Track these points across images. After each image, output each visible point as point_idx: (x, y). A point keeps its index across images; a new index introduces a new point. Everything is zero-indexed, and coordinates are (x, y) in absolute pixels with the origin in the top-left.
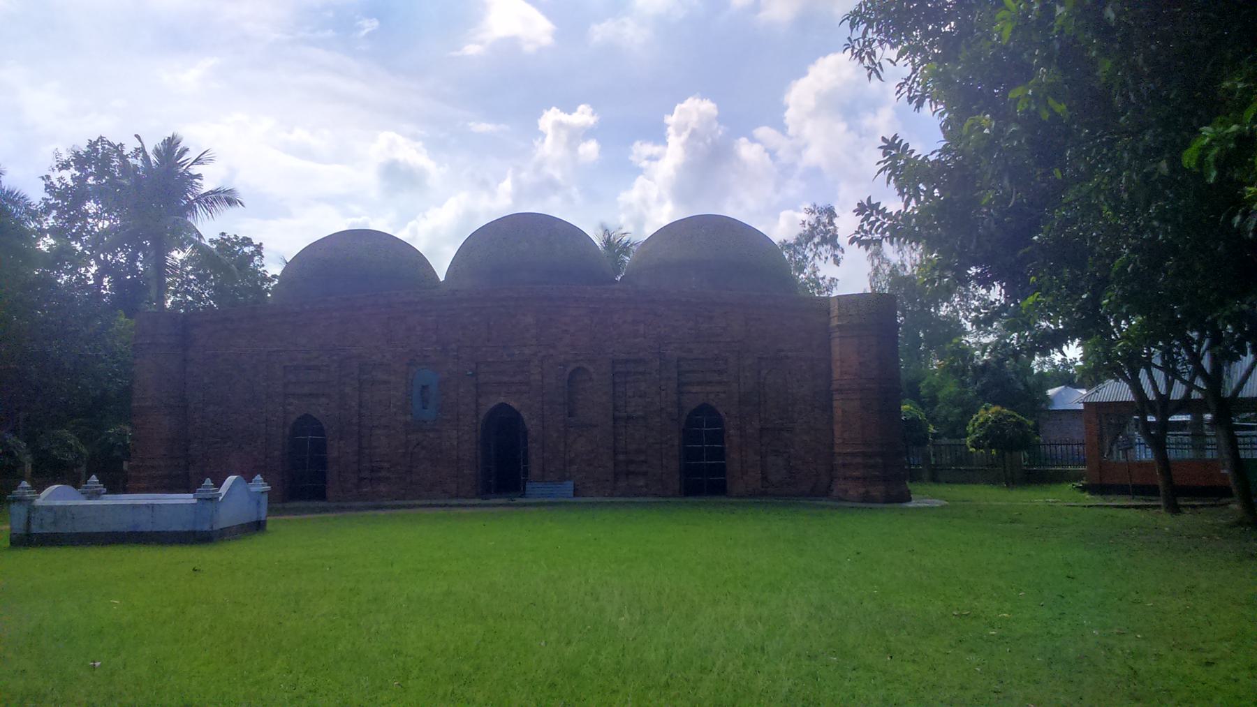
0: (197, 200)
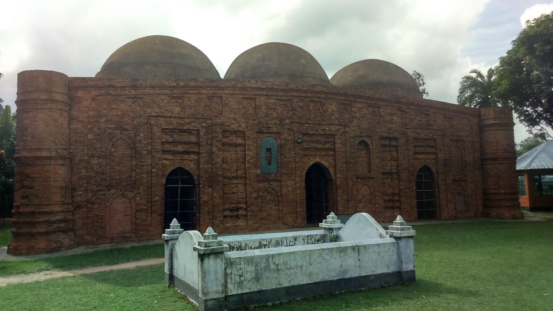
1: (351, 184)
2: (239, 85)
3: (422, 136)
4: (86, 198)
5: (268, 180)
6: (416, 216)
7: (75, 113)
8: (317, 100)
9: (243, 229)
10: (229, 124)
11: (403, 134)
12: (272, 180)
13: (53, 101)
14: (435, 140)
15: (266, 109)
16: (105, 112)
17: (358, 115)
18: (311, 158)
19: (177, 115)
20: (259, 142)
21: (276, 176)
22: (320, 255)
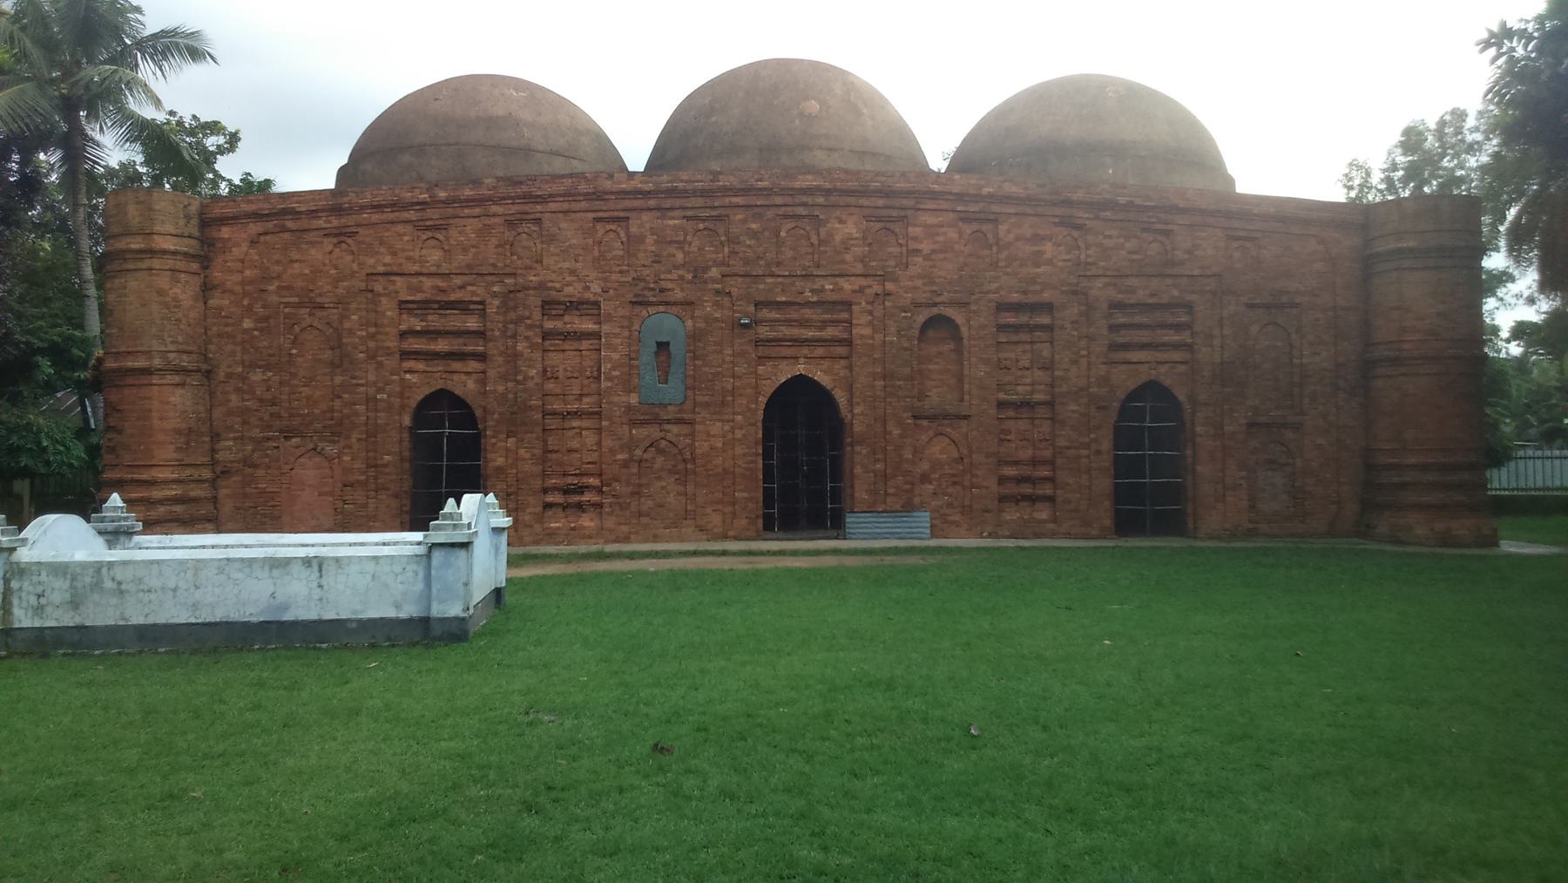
0: (141, 44)
1: (896, 432)
2: (583, 188)
3: (1141, 295)
4: (240, 455)
5: (656, 421)
6: (1108, 522)
7: (217, 275)
8: (801, 211)
9: (590, 537)
10: (558, 285)
11: (1074, 293)
12: (669, 422)
13: (152, 253)
14: (1189, 307)
15: (657, 242)
16: (278, 268)
17: (925, 247)
18: (783, 365)
19: (433, 269)
20: (636, 327)
21: (680, 411)
22: (221, 571)
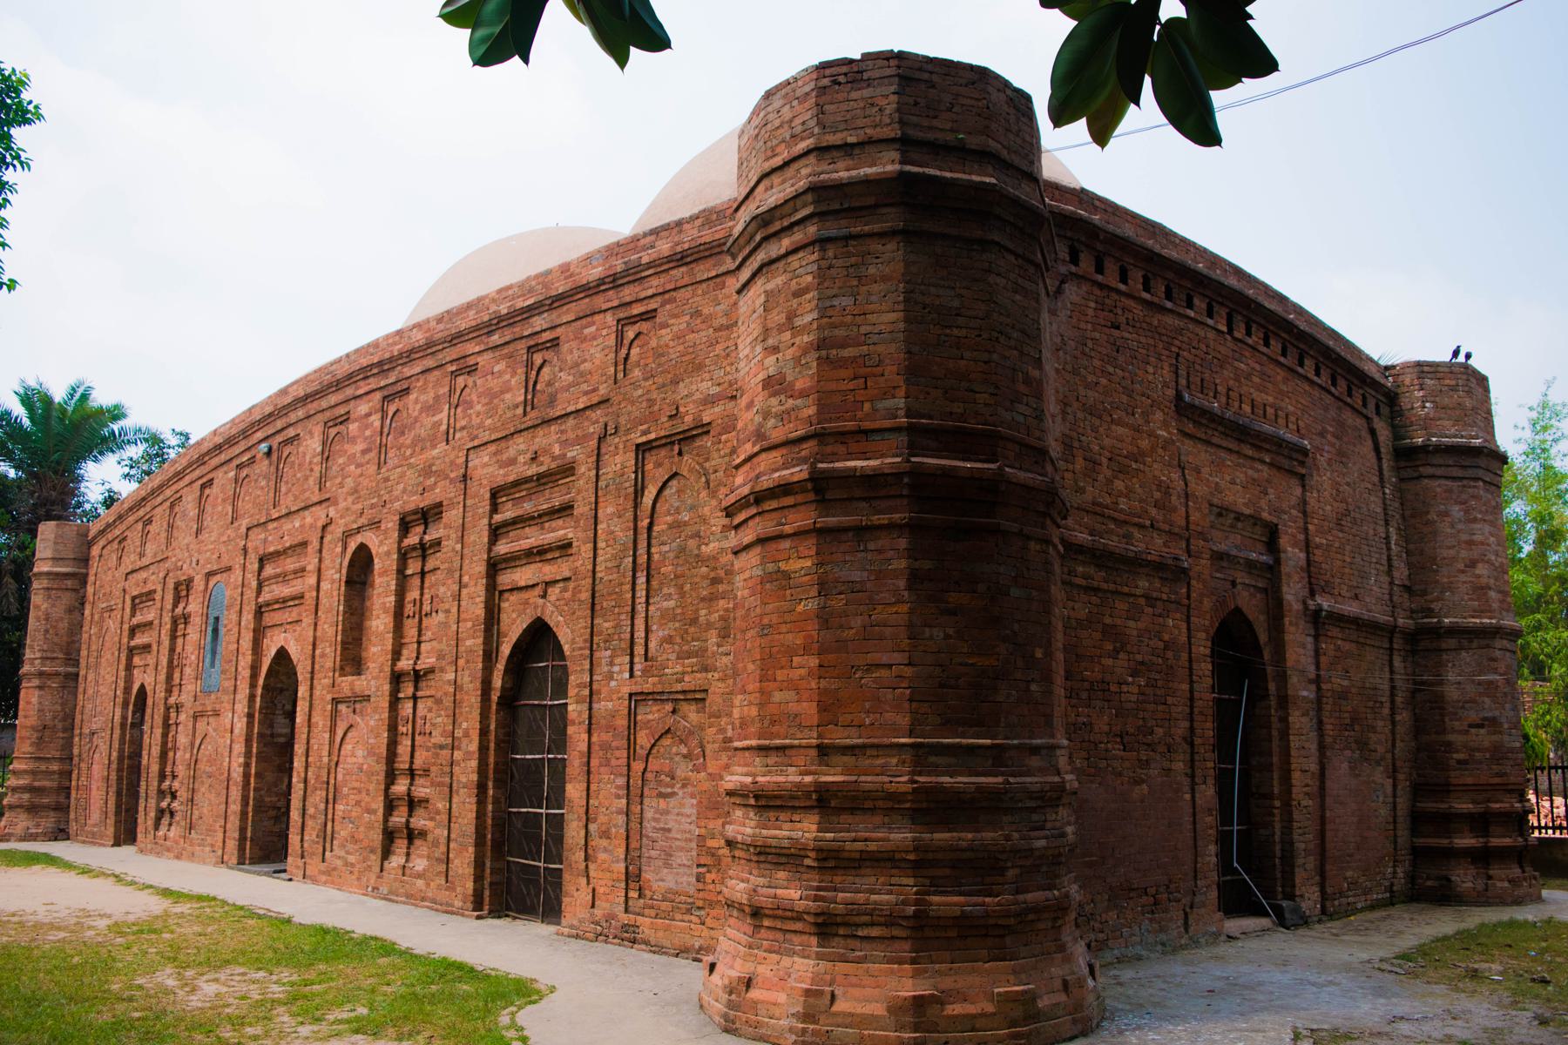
8: (291, 432)
